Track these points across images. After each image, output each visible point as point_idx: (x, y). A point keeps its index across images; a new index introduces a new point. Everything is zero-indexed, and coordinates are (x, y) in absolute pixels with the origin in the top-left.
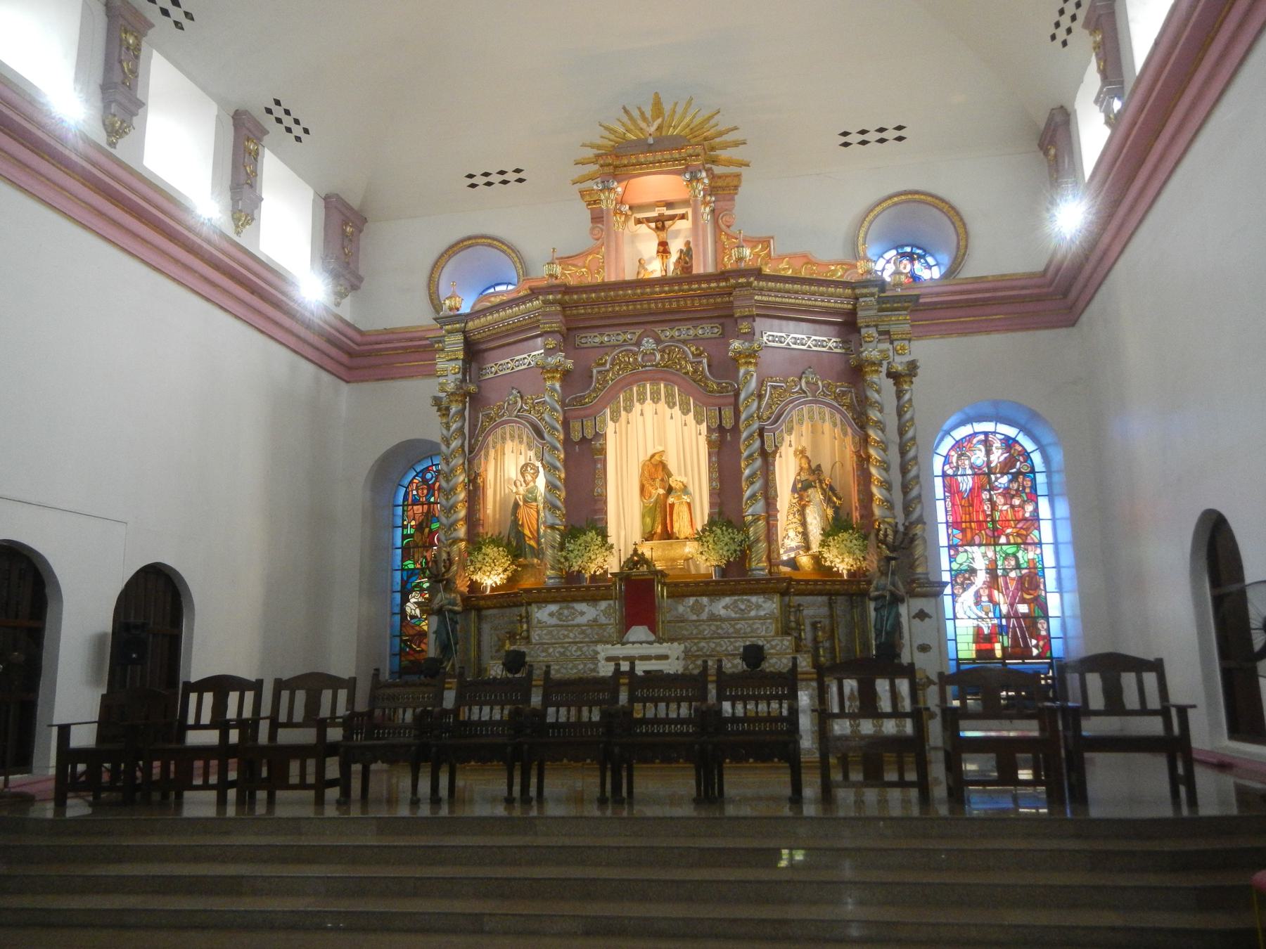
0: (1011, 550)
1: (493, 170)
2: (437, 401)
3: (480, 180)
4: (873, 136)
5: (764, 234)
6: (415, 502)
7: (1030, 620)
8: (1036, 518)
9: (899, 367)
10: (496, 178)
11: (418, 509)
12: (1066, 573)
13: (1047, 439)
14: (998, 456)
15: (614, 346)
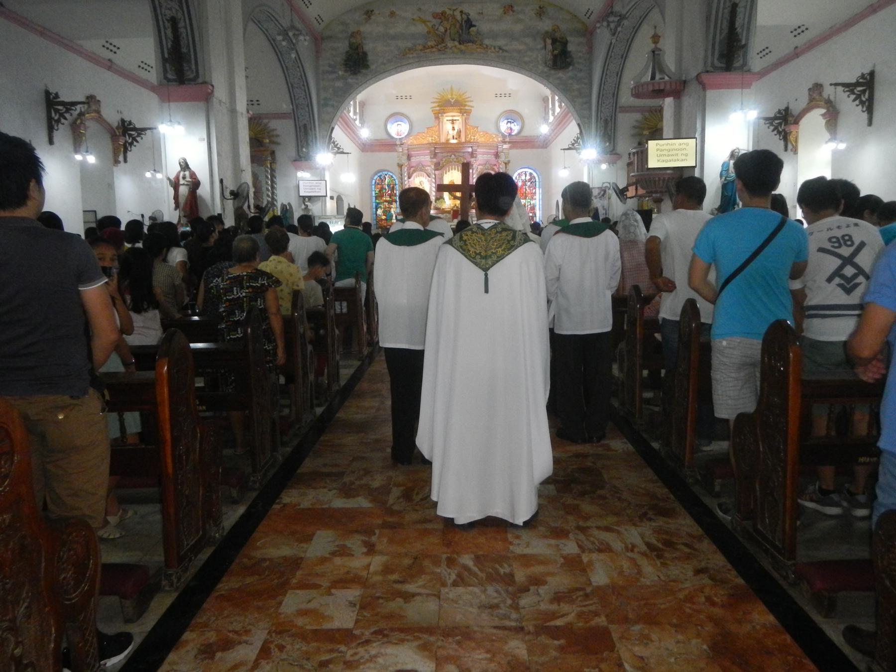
0: (529, 200)
1: (404, 95)
2: (398, 164)
3: (399, 97)
4: (503, 95)
5: (477, 126)
6: (378, 184)
7: (532, 217)
8: (535, 193)
9: (506, 162)
10: (404, 97)
11: (379, 186)
12: (541, 206)
13: (539, 174)
14: (528, 177)
15: (445, 157)
